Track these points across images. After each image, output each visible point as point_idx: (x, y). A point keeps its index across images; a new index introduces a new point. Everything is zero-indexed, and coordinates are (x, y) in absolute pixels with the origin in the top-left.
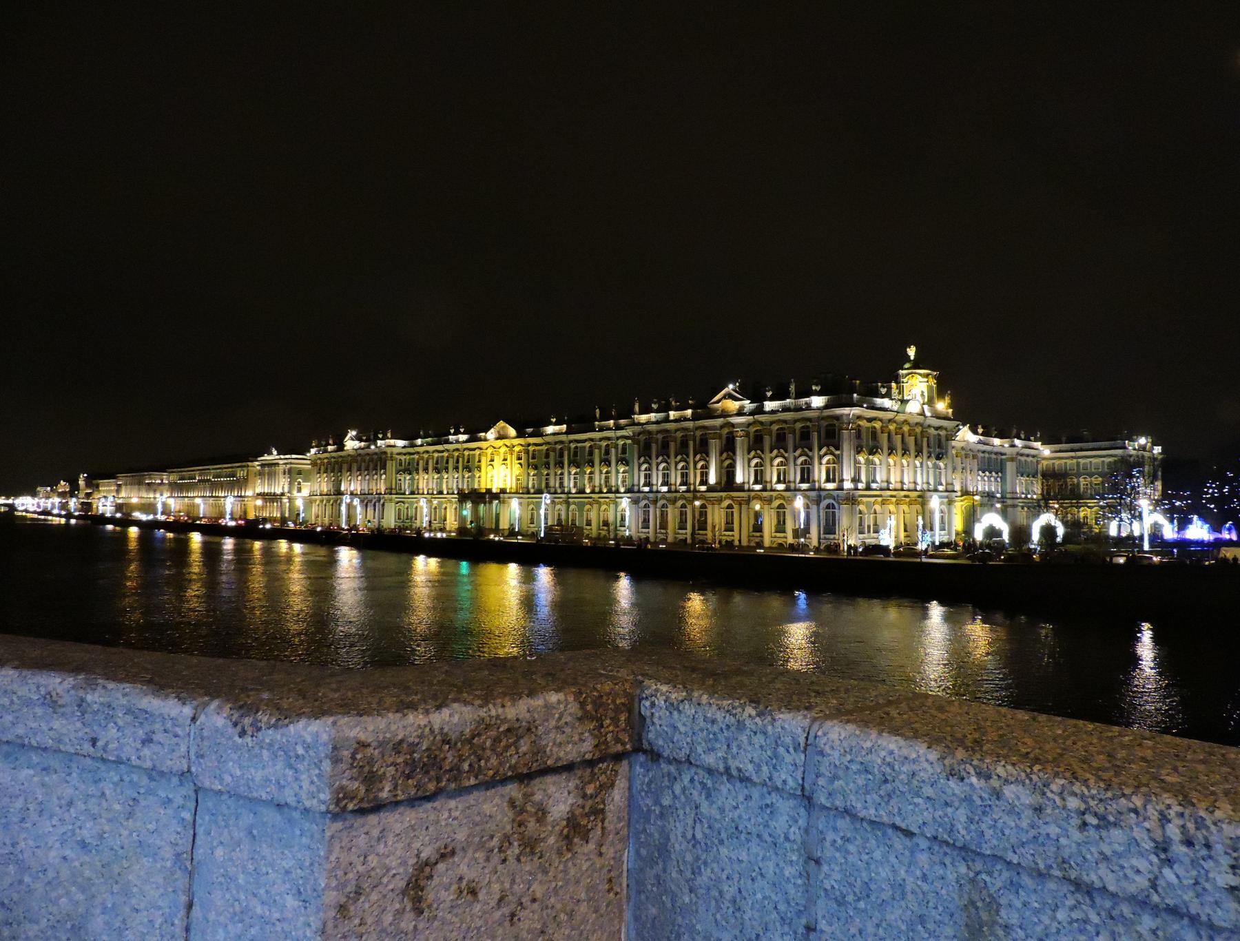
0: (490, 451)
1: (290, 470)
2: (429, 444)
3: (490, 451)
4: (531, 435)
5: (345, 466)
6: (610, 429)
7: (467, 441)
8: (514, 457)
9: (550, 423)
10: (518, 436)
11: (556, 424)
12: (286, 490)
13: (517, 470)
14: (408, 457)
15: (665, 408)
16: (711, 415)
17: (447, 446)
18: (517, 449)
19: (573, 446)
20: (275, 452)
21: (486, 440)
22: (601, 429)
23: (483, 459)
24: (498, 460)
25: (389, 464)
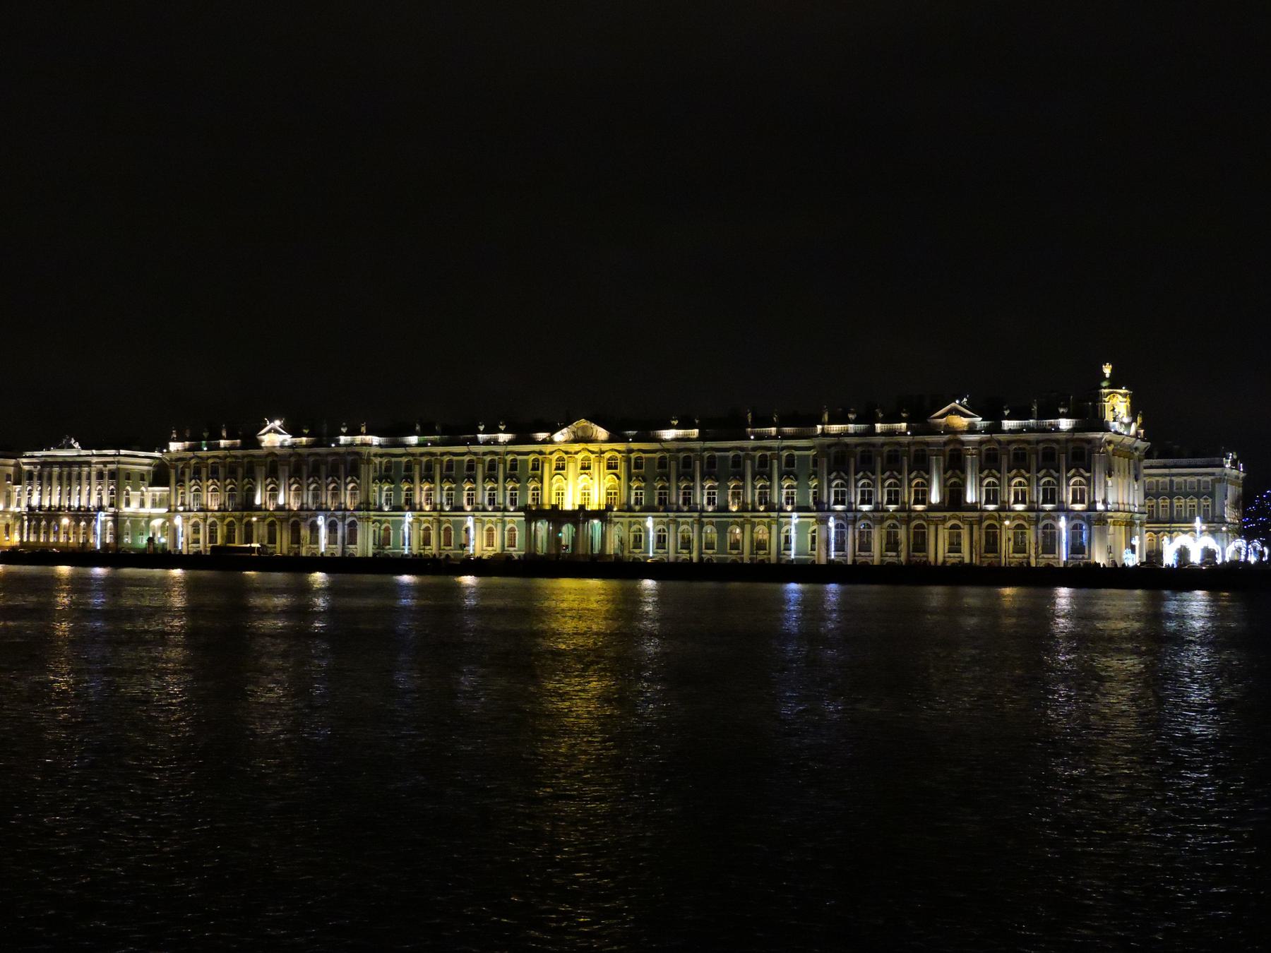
0: (555, 456)
1: (113, 475)
2: (434, 444)
3: (555, 456)
4: (636, 440)
5: (260, 472)
6: (770, 437)
7: (510, 443)
8: (604, 465)
9: (670, 427)
10: (610, 440)
11: (677, 427)
12: (106, 502)
13: (609, 480)
14: (385, 460)
15: (868, 418)
16: (934, 430)
17: (474, 448)
18: (607, 455)
19: (706, 454)
20: (77, 445)
21: (551, 442)
22: (759, 437)
23: (546, 466)
24: (572, 469)
25: (363, 468)
